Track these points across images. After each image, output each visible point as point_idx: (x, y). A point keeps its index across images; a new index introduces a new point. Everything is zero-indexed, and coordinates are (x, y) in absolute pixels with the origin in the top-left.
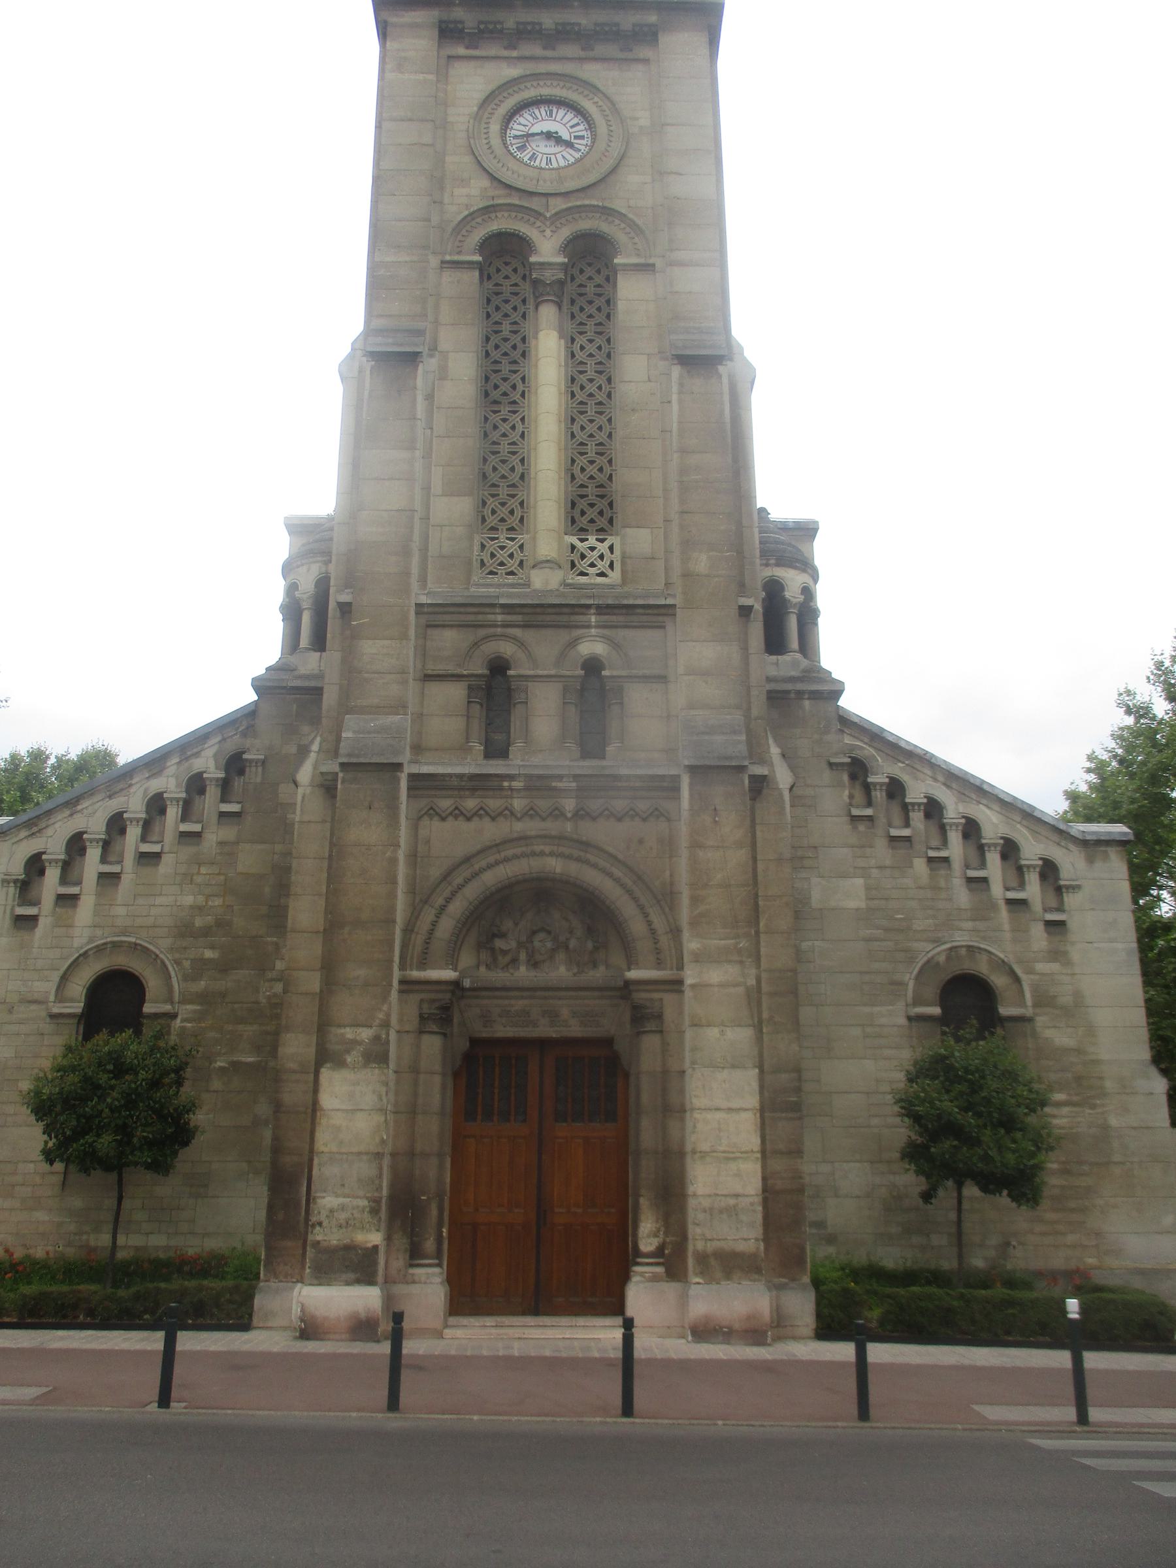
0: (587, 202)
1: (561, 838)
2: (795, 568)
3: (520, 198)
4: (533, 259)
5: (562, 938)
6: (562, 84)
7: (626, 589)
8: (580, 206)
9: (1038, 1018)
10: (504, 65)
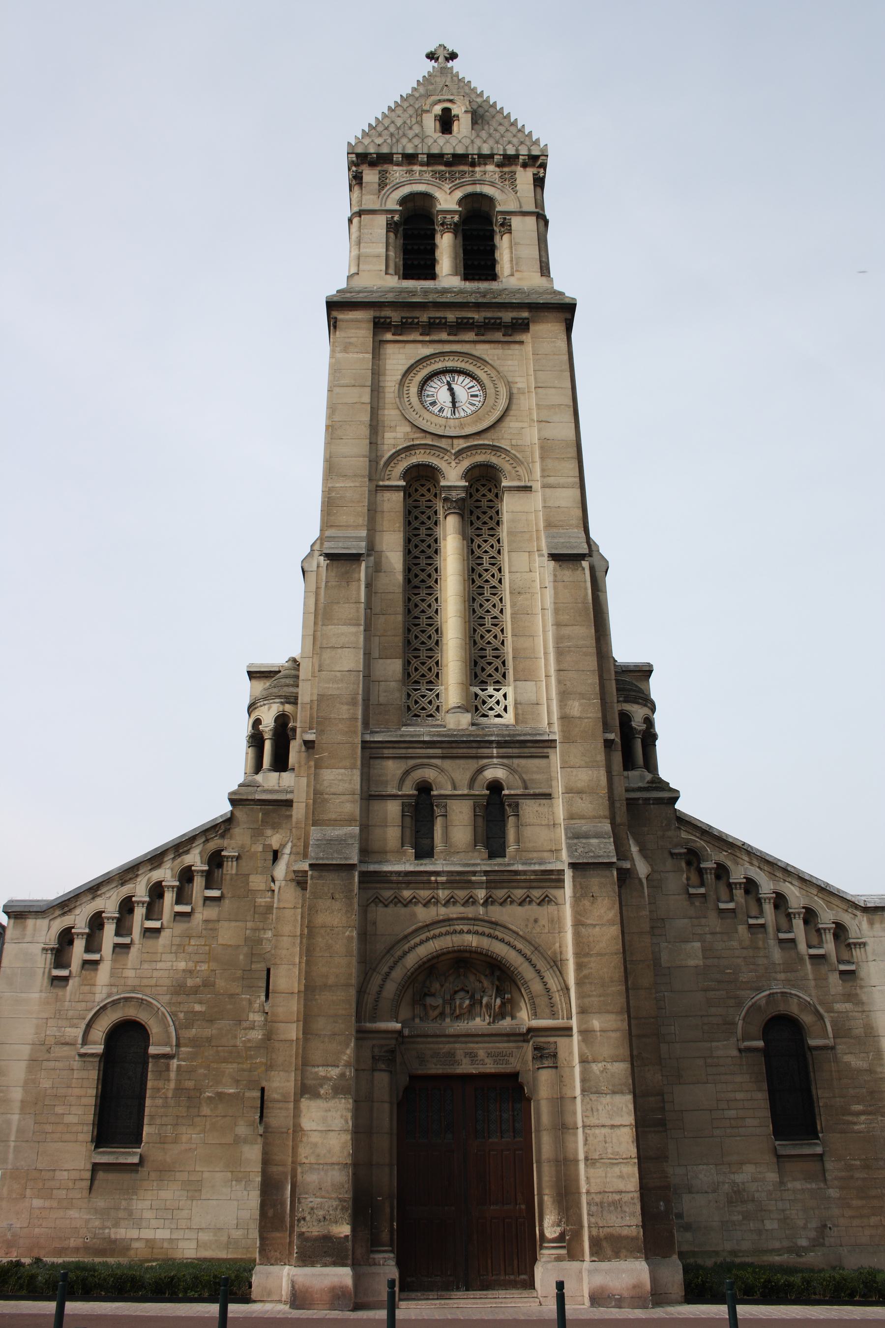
4: (442, 484)
5: (477, 997)
6: (461, 359)
8: (476, 445)
10: (420, 346)
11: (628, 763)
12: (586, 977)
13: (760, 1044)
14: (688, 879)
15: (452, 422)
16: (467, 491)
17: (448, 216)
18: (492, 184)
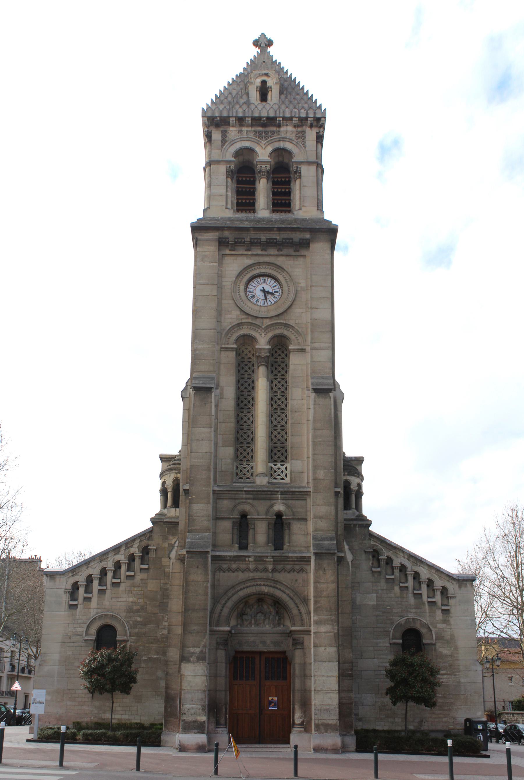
0: (279, 321)
1: (268, 579)
3: (252, 319)
4: (257, 347)
5: (267, 616)
6: (269, 267)
7: (292, 485)
8: (276, 323)
9: (437, 644)
10: (245, 258)
11: (347, 506)
12: (319, 607)
13: (401, 641)
14: (372, 564)
15: (263, 309)
16: (270, 352)
17: (264, 166)
18: (291, 141)
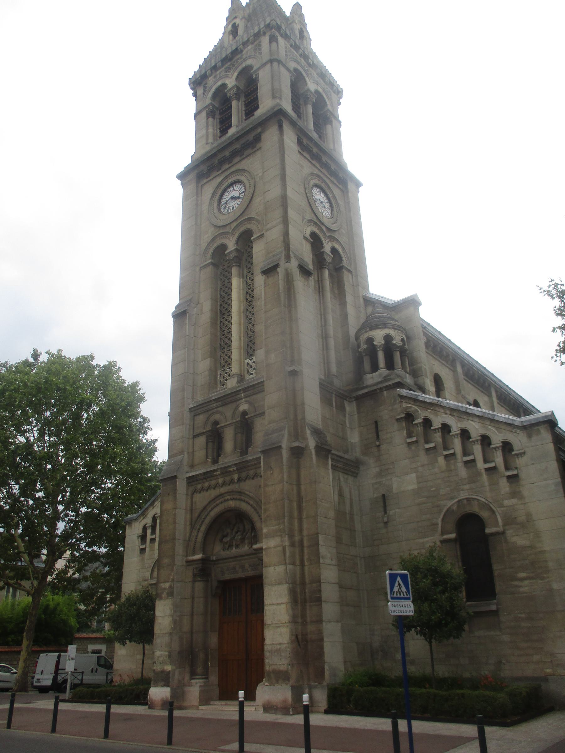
2: (380, 328)
